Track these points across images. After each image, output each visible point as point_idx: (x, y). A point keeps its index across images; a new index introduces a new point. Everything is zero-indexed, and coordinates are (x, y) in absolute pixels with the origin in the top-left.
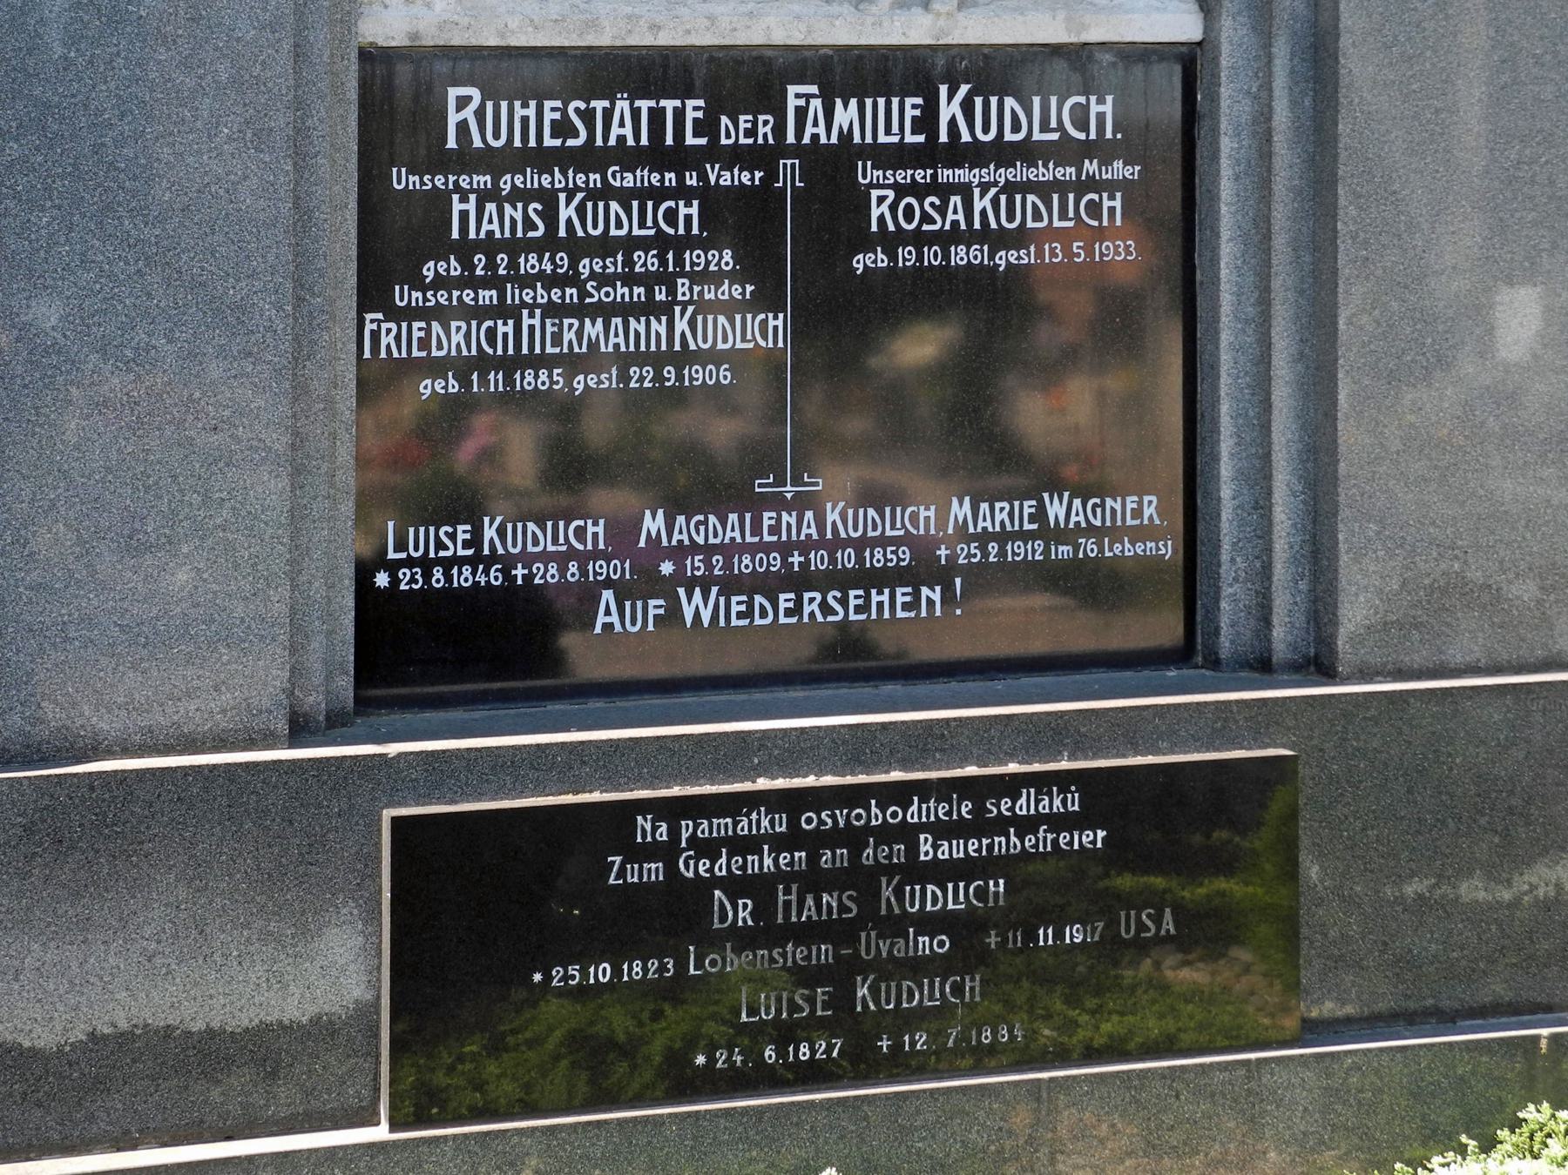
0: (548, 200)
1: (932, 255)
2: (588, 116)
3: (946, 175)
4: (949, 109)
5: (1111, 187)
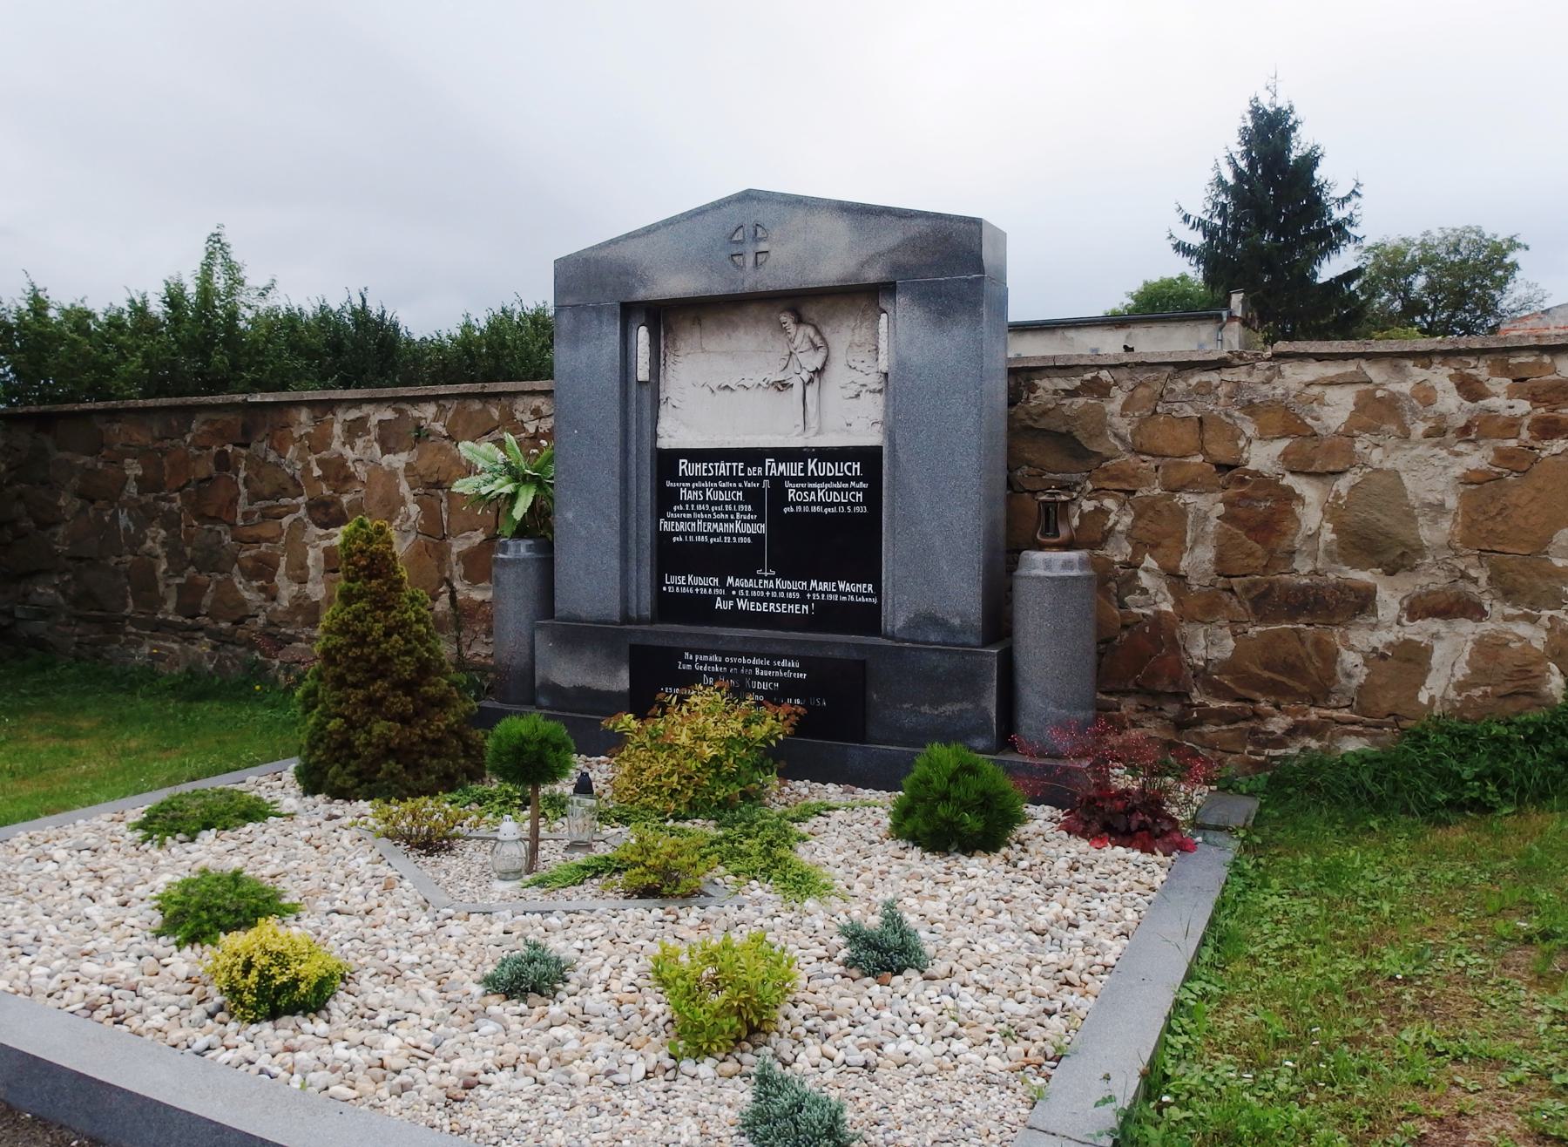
0: (704, 489)
1: (806, 509)
2: (714, 467)
3: (810, 485)
4: (811, 466)
5: (859, 490)
